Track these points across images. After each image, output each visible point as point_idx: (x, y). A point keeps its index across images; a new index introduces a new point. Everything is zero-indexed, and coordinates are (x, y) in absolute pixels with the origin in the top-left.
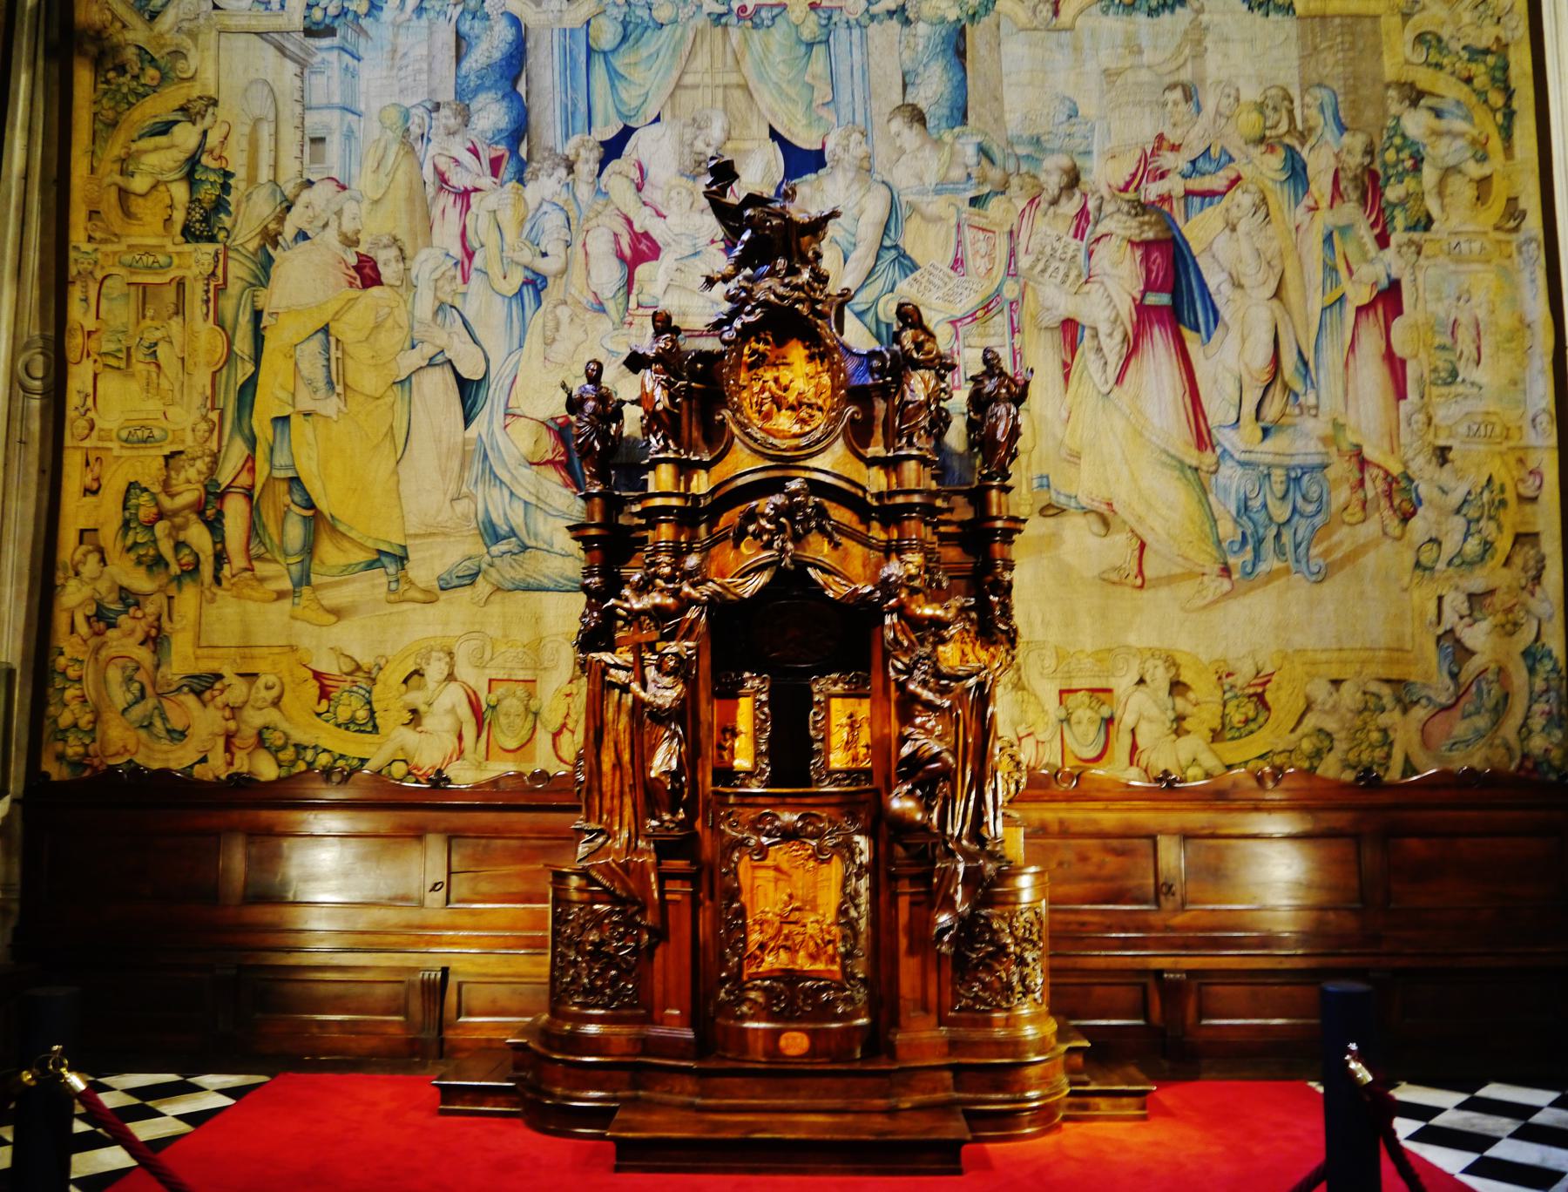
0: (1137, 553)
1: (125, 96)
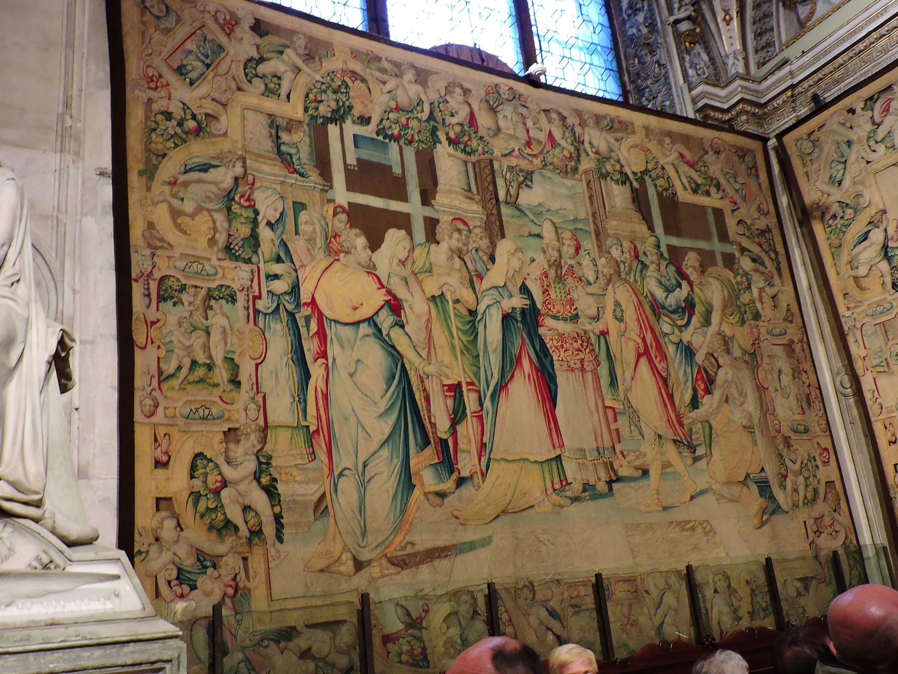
1: (840, 230)
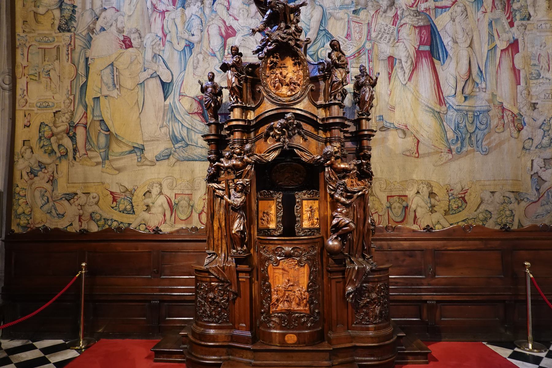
0: (416, 145)
